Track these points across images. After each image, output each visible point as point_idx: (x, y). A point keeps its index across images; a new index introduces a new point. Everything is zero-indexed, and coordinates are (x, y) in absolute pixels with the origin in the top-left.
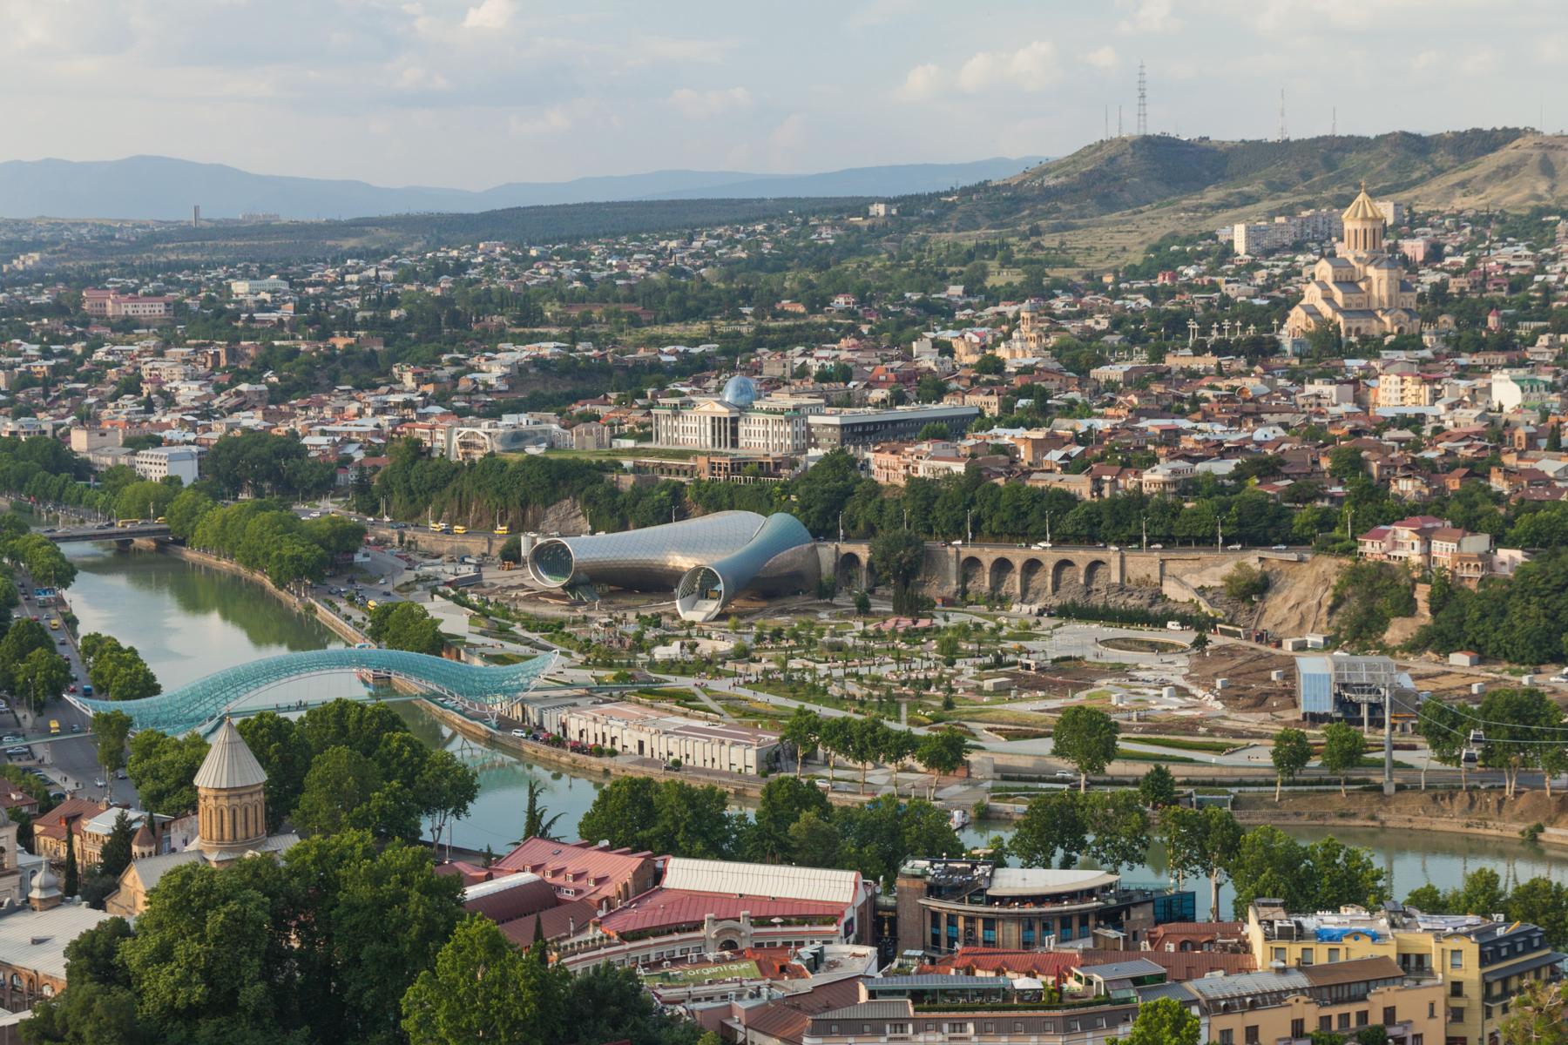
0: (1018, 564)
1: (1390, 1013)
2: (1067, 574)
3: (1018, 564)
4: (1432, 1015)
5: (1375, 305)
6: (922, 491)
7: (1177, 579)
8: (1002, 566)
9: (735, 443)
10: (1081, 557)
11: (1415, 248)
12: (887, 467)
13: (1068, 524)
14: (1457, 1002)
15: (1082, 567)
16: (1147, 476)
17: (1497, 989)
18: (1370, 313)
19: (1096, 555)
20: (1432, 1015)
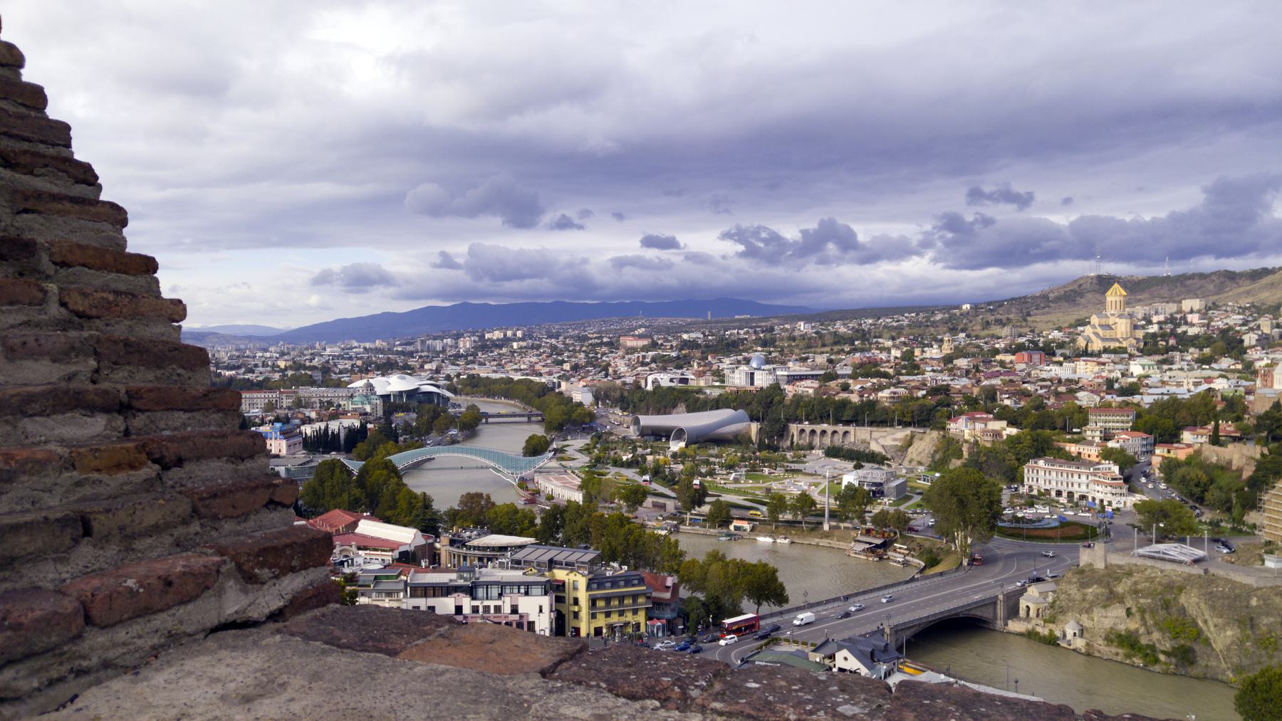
0: (818, 432)
1: (514, 610)
2: (836, 437)
3: (818, 432)
4: (541, 611)
5: (1119, 336)
6: (798, 399)
7: (876, 440)
8: (813, 432)
9: (752, 383)
10: (841, 428)
11: (1194, 318)
12: (790, 390)
13: (847, 414)
14: (576, 609)
15: (841, 433)
16: (880, 394)
17: (601, 604)
18: (1117, 340)
19: (846, 428)
20: (541, 611)
